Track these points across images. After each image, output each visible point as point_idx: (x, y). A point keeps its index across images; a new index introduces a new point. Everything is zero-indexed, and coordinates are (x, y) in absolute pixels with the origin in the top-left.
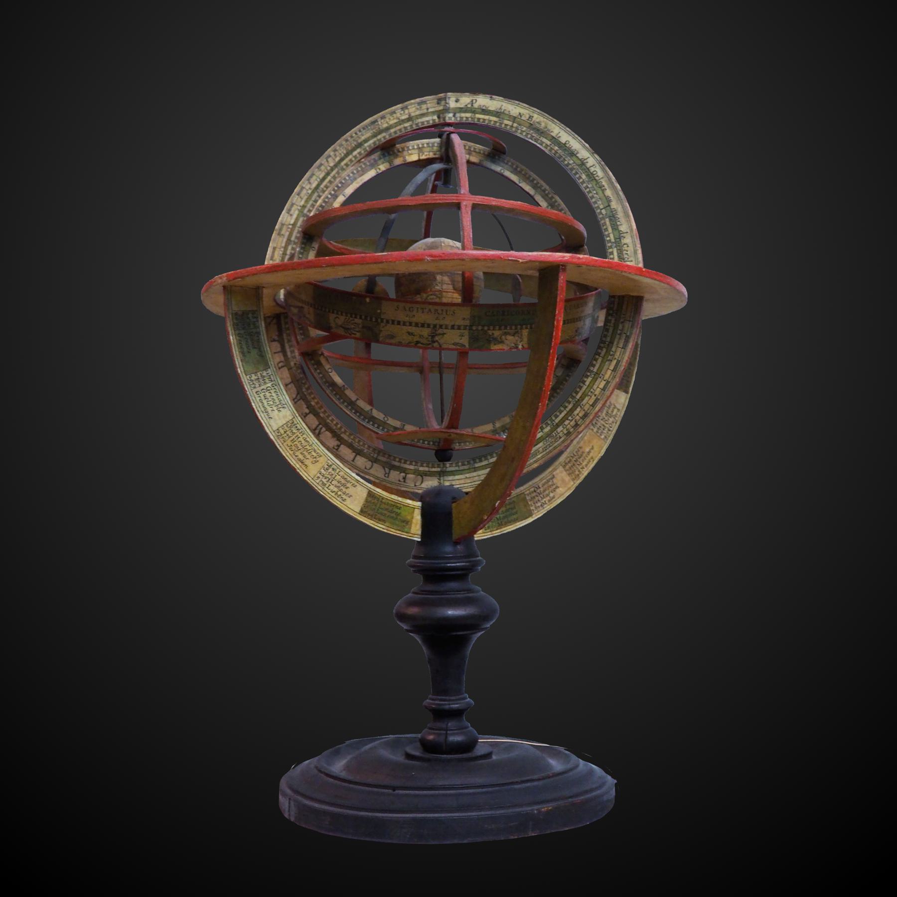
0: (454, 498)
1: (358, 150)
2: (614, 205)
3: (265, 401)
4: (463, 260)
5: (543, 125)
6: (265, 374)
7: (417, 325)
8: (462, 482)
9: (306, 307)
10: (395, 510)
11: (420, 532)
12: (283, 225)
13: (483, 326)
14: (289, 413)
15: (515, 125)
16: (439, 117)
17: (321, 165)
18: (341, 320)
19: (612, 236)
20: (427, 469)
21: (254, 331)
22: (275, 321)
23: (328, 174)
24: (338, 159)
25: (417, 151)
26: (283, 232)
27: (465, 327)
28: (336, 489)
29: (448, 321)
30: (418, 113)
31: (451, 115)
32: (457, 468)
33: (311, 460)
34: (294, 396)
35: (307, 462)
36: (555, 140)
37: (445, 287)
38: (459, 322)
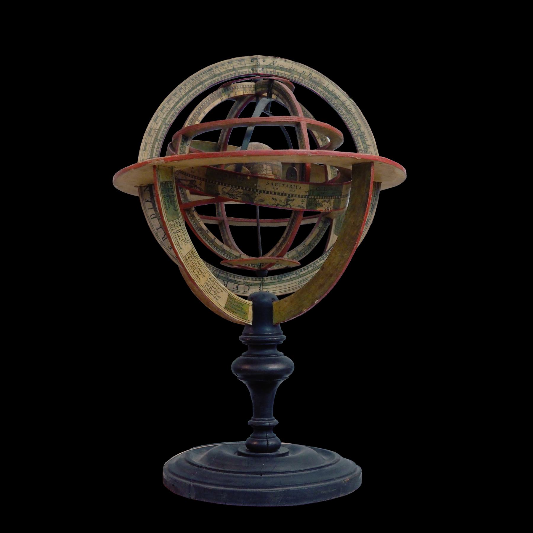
0: (273, 299)
1: (201, 86)
2: (363, 129)
3: (178, 238)
4: (329, 156)
5: (318, 79)
6: (177, 221)
7: (279, 194)
8: (274, 289)
9: (198, 182)
10: (241, 306)
11: (252, 320)
12: (151, 129)
13: (315, 196)
14: (190, 246)
15: (301, 78)
16: (253, 70)
17: (176, 93)
18: (228, 189)
19: (362, 146)
20: (252, 282)
21: (171, 194)
22: (148, 189)
23: (181, 99)
24: (187, 91)
25: (242, 89)
26: (152, 134)
27: (305, 196)
28: (213, 293)
29: (297, 192)
30: (239, 66)
31: (261, 69)
32: (271, 281)
33: (202, 275)
34: (163, 236)
35: (200, 276)
36: (325, 89)
37: (268, 172)
38: (303, 193)
